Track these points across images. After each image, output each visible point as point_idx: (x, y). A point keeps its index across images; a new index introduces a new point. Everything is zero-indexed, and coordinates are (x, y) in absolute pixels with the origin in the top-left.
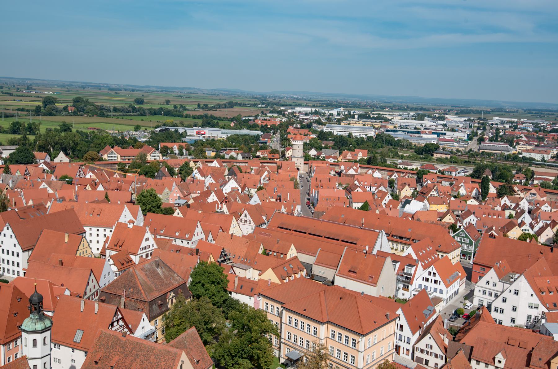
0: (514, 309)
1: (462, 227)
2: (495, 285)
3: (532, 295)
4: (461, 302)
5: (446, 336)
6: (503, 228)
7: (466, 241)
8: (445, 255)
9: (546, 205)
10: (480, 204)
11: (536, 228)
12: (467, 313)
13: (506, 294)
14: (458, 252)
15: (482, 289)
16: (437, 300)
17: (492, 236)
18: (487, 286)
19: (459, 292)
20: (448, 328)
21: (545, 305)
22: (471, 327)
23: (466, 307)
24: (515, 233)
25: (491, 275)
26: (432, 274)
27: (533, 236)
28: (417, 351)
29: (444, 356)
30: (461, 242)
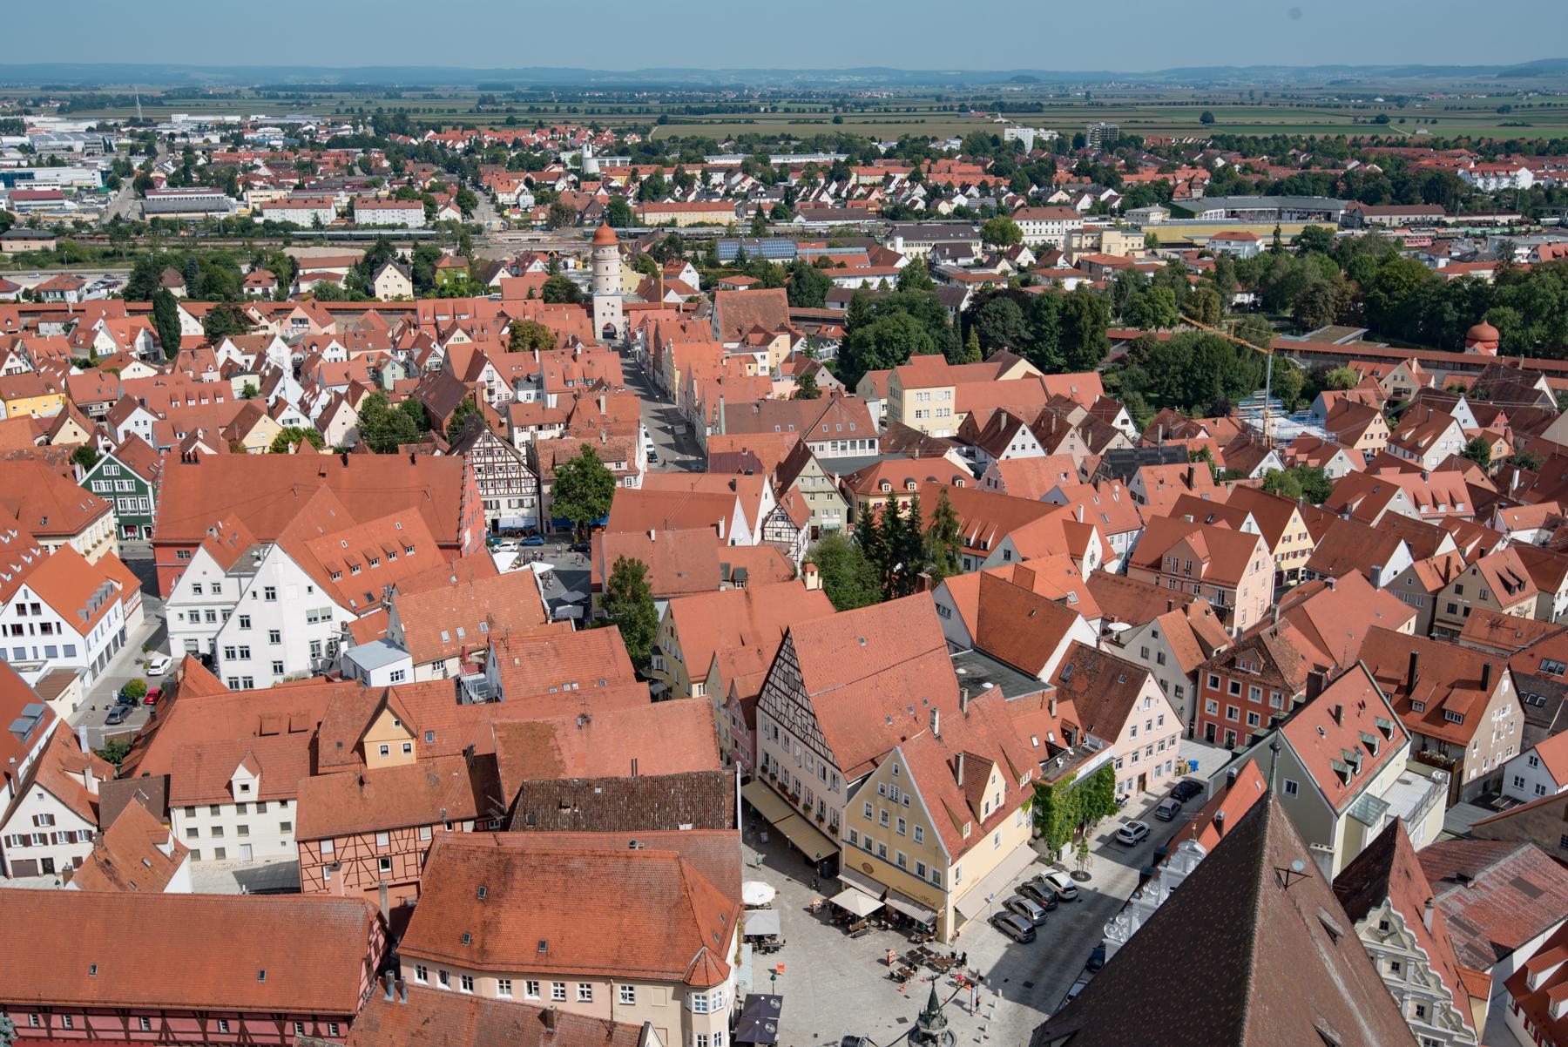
0: (275, 637)
1: (114, 448)
2: (217, 589)
3: (310, 589)
4: (138, 662)
5: (89, 772)
6: (230, 428)
7: (127, 486)
8: (60, 542)
9: (334, 344)
10: (161, 372)
11: (316, 412)
12: (154, 686)
13: (246, 607)
14: (109, 521)
15: (185, 611)
16: (58, 682)
17: (193, 459)
18: (198, 598)
19: (129, 634)
20: (102, 746)
21: (345, 604)
22: (156, 724)
23: (152, 672)
24: (261, 436)
25: (202, 565)
26: (28, 608)
27: (308, 433)
28: (9, 845)
29: (94, 830)
30: (115, 494)
